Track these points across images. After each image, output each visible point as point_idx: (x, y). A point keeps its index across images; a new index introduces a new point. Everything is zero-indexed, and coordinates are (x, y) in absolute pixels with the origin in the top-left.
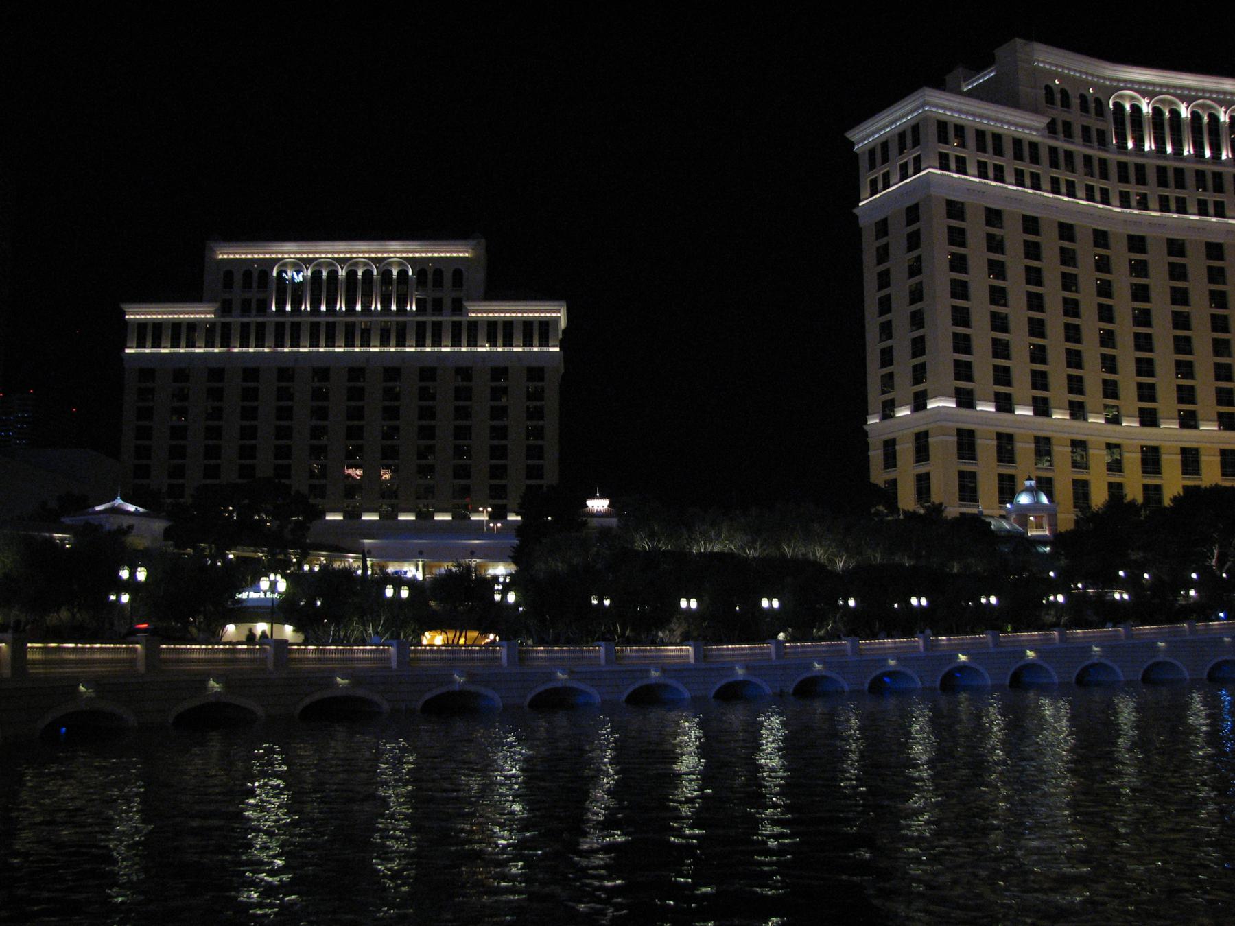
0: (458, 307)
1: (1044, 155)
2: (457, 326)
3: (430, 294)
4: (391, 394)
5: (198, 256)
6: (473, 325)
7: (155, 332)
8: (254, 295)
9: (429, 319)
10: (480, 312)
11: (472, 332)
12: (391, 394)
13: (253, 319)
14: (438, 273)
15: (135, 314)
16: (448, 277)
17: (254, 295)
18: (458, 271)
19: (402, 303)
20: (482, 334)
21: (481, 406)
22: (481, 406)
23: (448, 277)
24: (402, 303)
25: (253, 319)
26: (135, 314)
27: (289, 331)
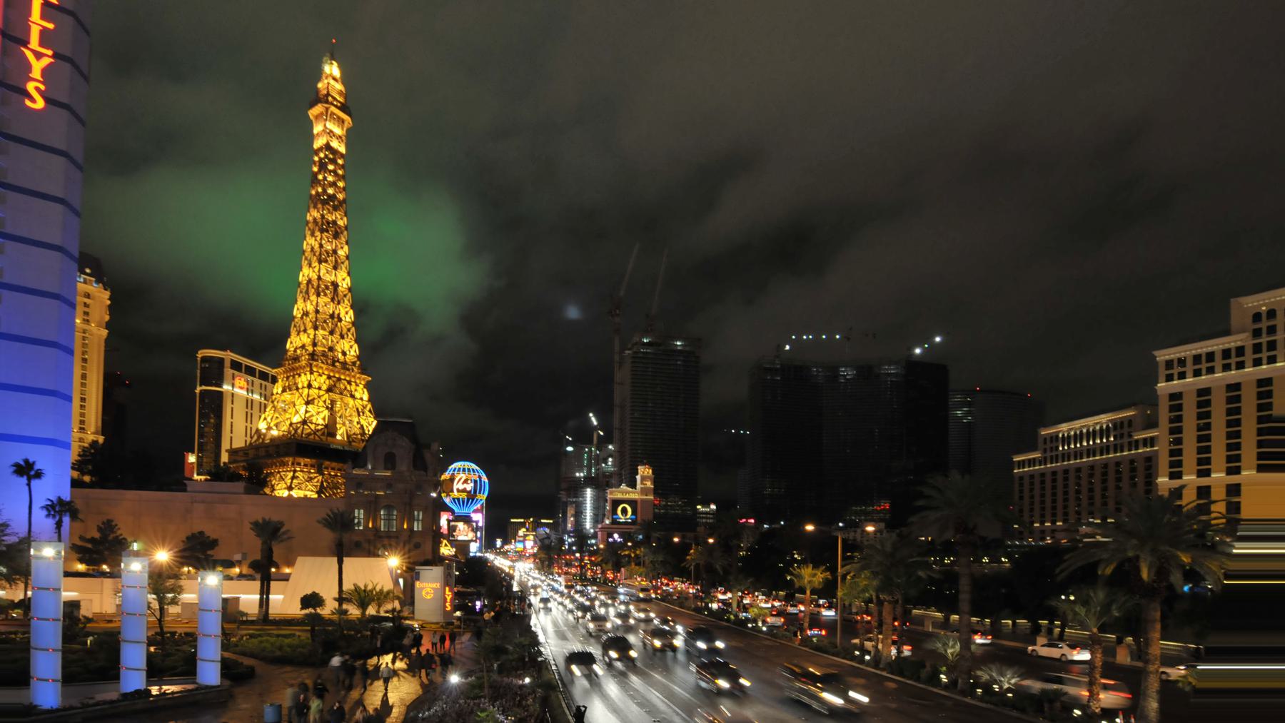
0: (1130, 436)
1: (1249, 351)
2: (1130, 443)
3: (1118, 433)
4: (1118, 472)
5: (1035, 435)
6: (1137, 441)
7: (1022, 464)
8: (1054, 445)
9: (1119, 442)
10: (1139, 436)
11: (1136, 444)
12: (1118, 472)
13: (1054, 454)
14: (1122, 423)
15: (1016, 459)
16: (1126, 424)
17: (1054, 445)
18: (1130, 421)
19: (1108, 438)
20: (1141, 444)
21: (1048, 484)
22: (1048, 484)
23: (1126, 424)
24: (1108, 438)
25: (1054, 454)
26: (1016, 459)
27: (1066, 456)
